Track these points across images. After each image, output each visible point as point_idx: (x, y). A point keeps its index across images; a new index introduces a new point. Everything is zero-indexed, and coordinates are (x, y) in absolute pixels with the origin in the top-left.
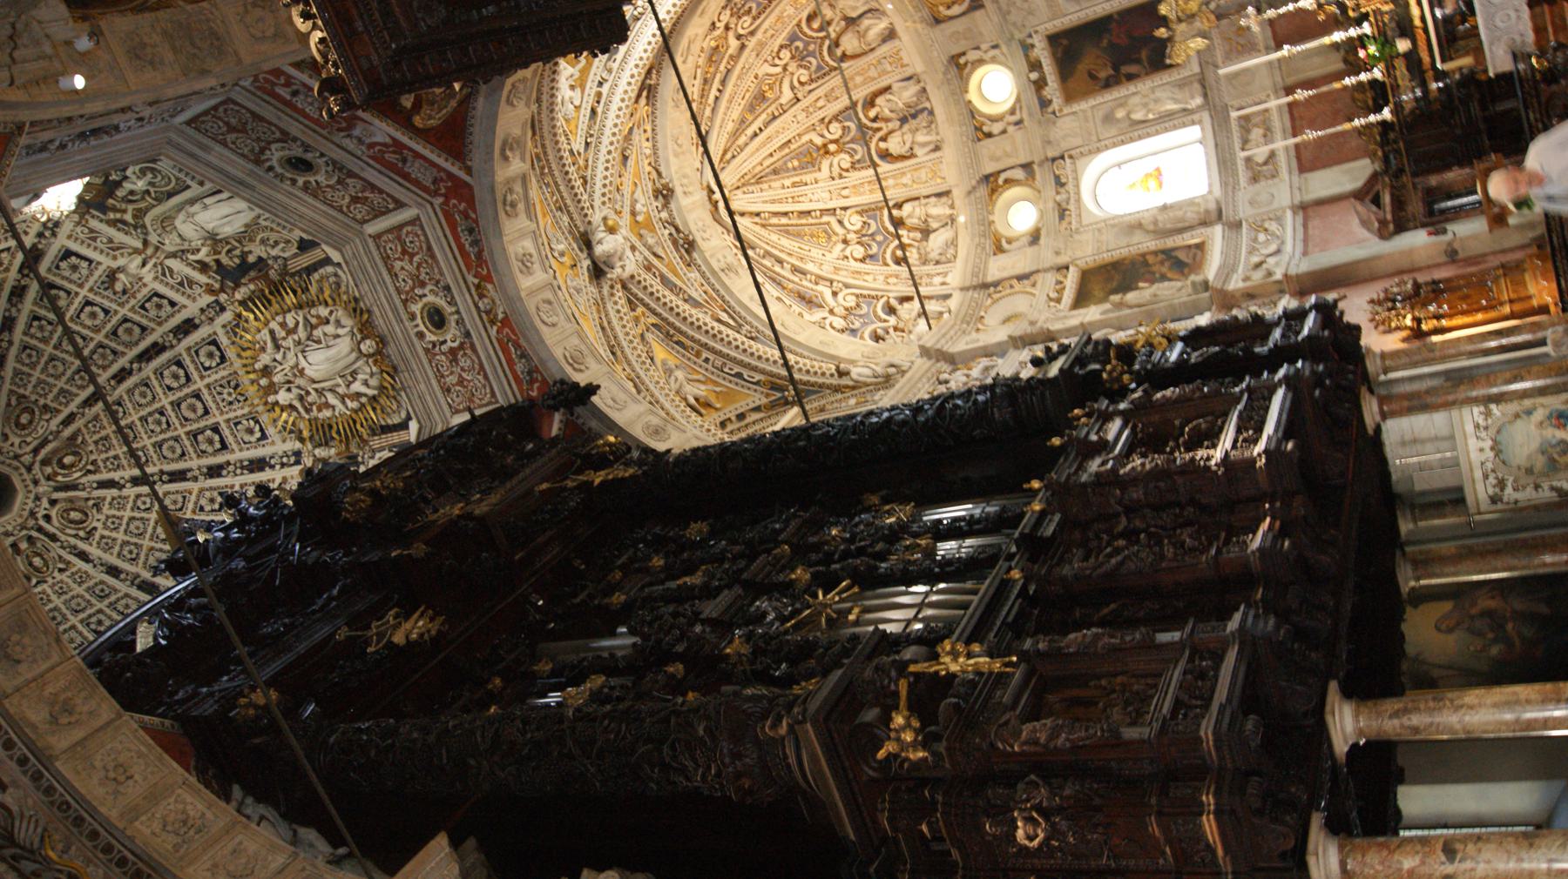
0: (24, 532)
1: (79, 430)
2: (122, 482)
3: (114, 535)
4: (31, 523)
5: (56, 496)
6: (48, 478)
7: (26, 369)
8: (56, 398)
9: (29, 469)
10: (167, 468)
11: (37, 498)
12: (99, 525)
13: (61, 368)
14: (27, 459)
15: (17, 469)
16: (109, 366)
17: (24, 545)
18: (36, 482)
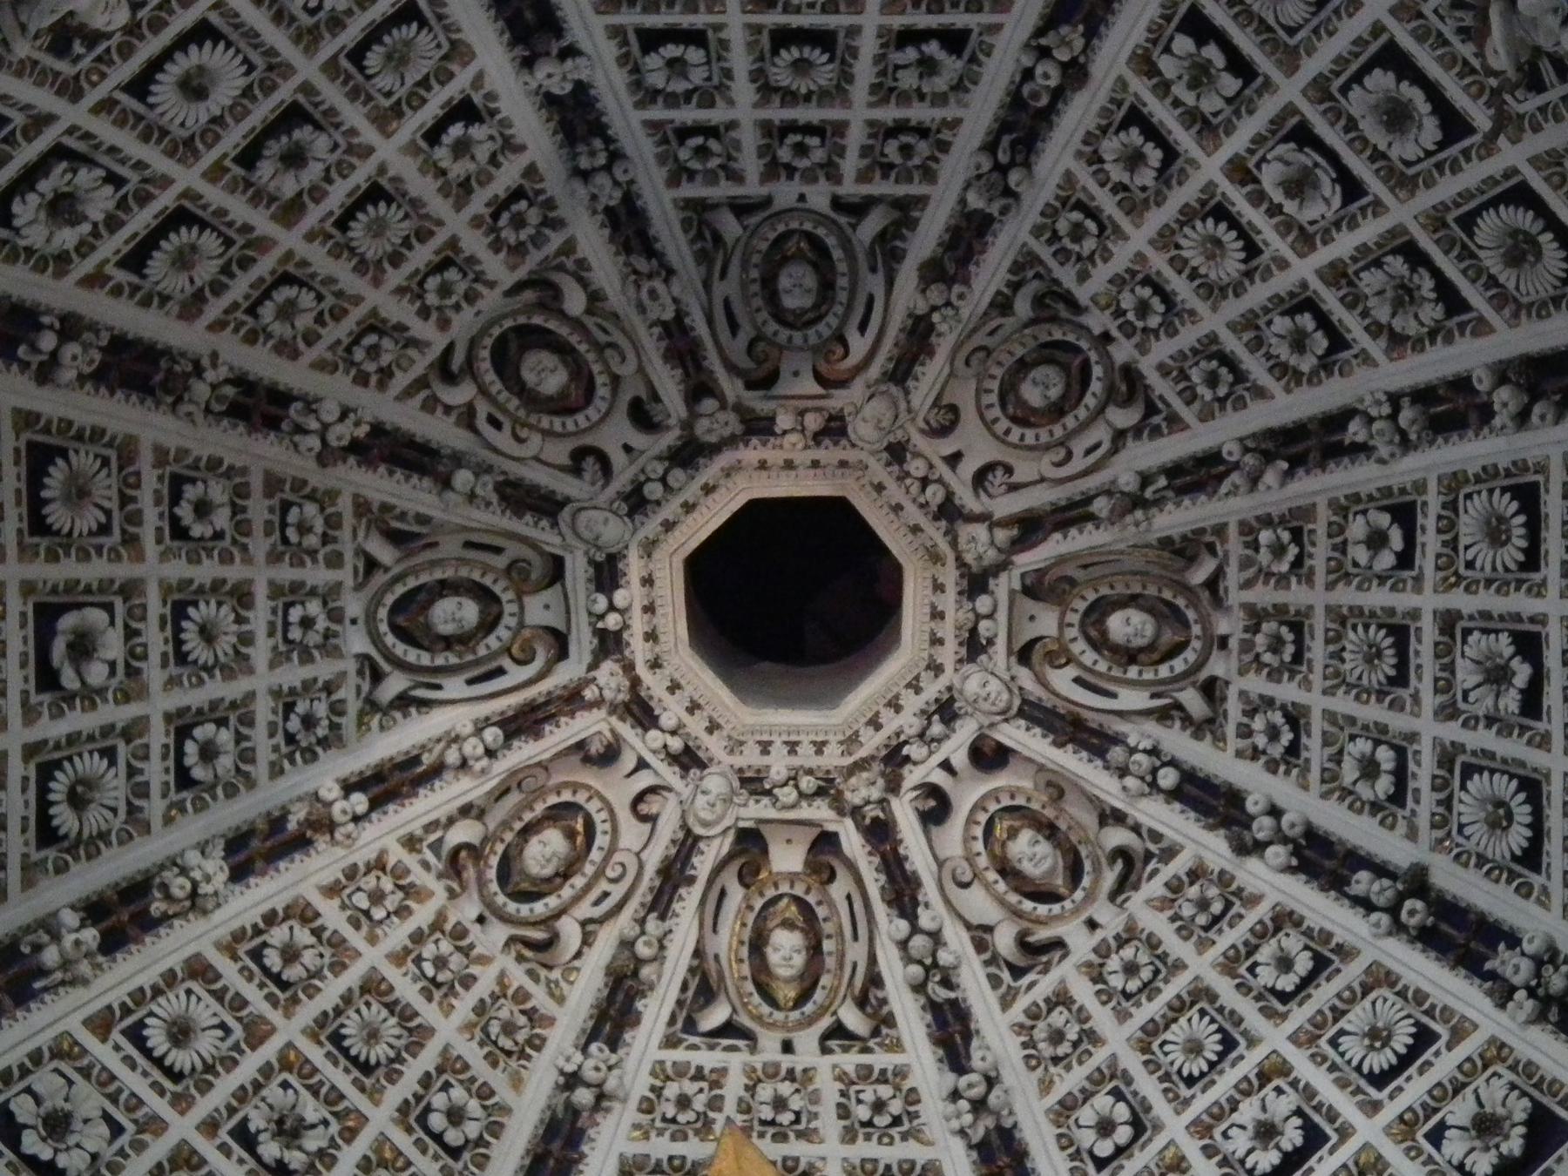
0: (821, 812)
1: (1220, 530)
2: (1263, 827)
3: (1102, 1018)
4: (863, 790)
5: (1015, 735)
6: (1024, 655)
7: (1107, 203)
8: (1176, 370)
9: (976, 583)
10: (1452, 879)
11: (947, 710)
12: (1081, 944)
13: (1232, 265)
14: (979, 542)
15: (935, 557)
16: (1418, 345)
17: (787, 858)
18: (974, 647)
